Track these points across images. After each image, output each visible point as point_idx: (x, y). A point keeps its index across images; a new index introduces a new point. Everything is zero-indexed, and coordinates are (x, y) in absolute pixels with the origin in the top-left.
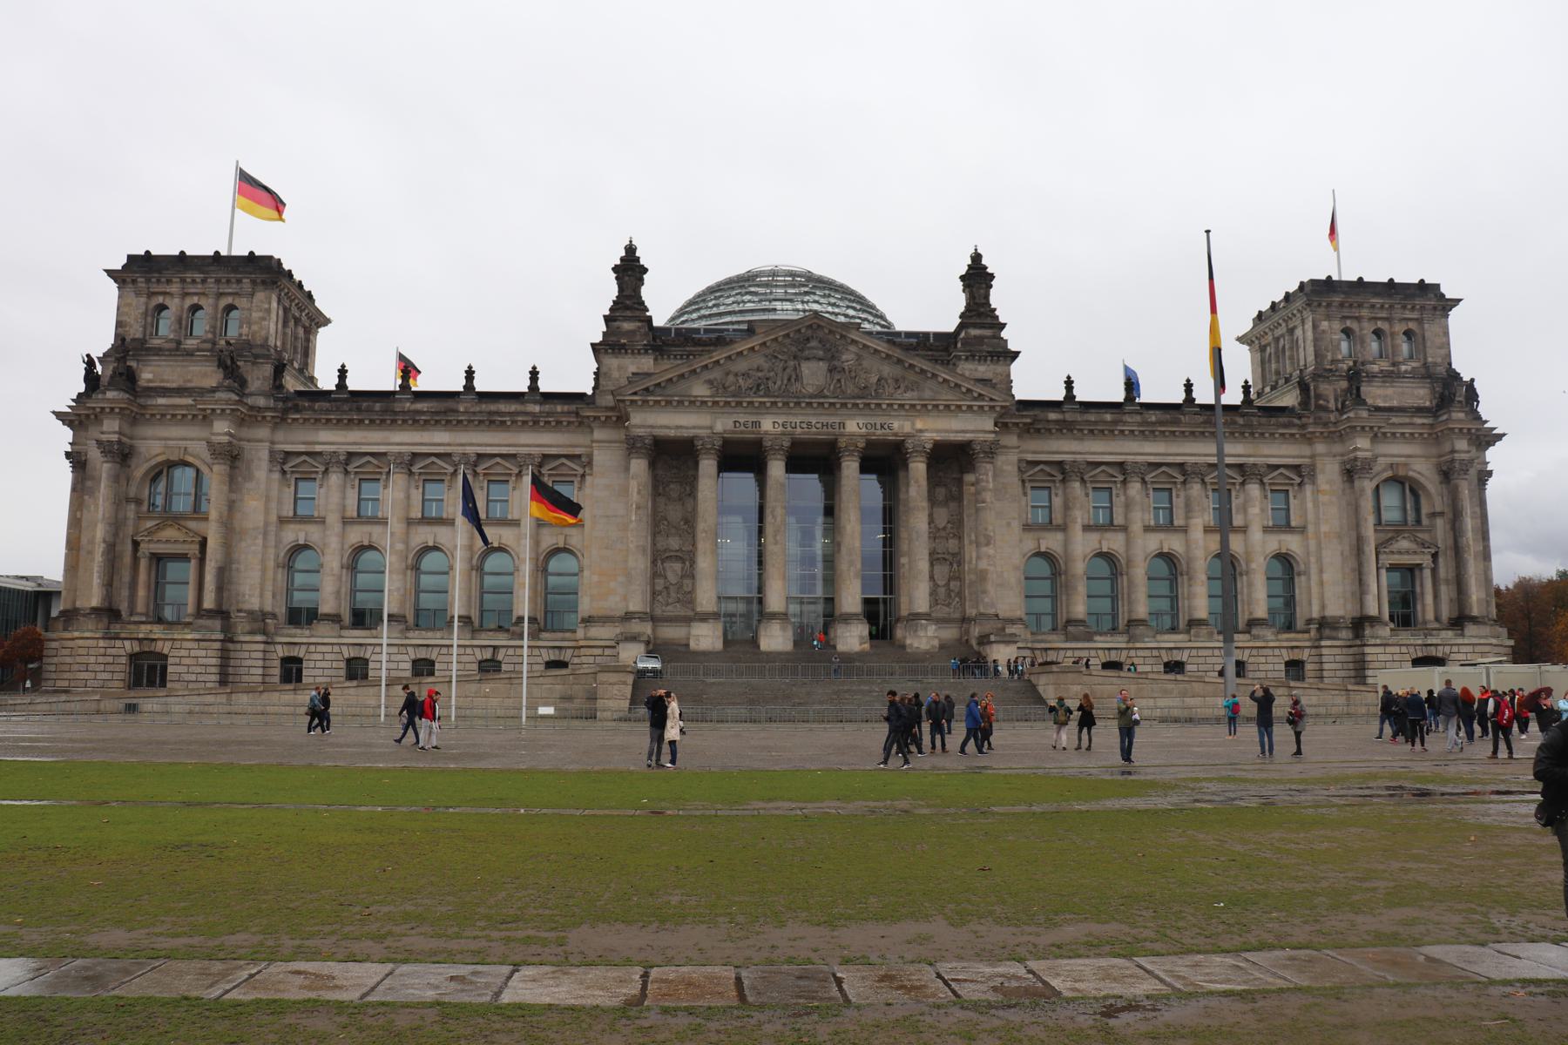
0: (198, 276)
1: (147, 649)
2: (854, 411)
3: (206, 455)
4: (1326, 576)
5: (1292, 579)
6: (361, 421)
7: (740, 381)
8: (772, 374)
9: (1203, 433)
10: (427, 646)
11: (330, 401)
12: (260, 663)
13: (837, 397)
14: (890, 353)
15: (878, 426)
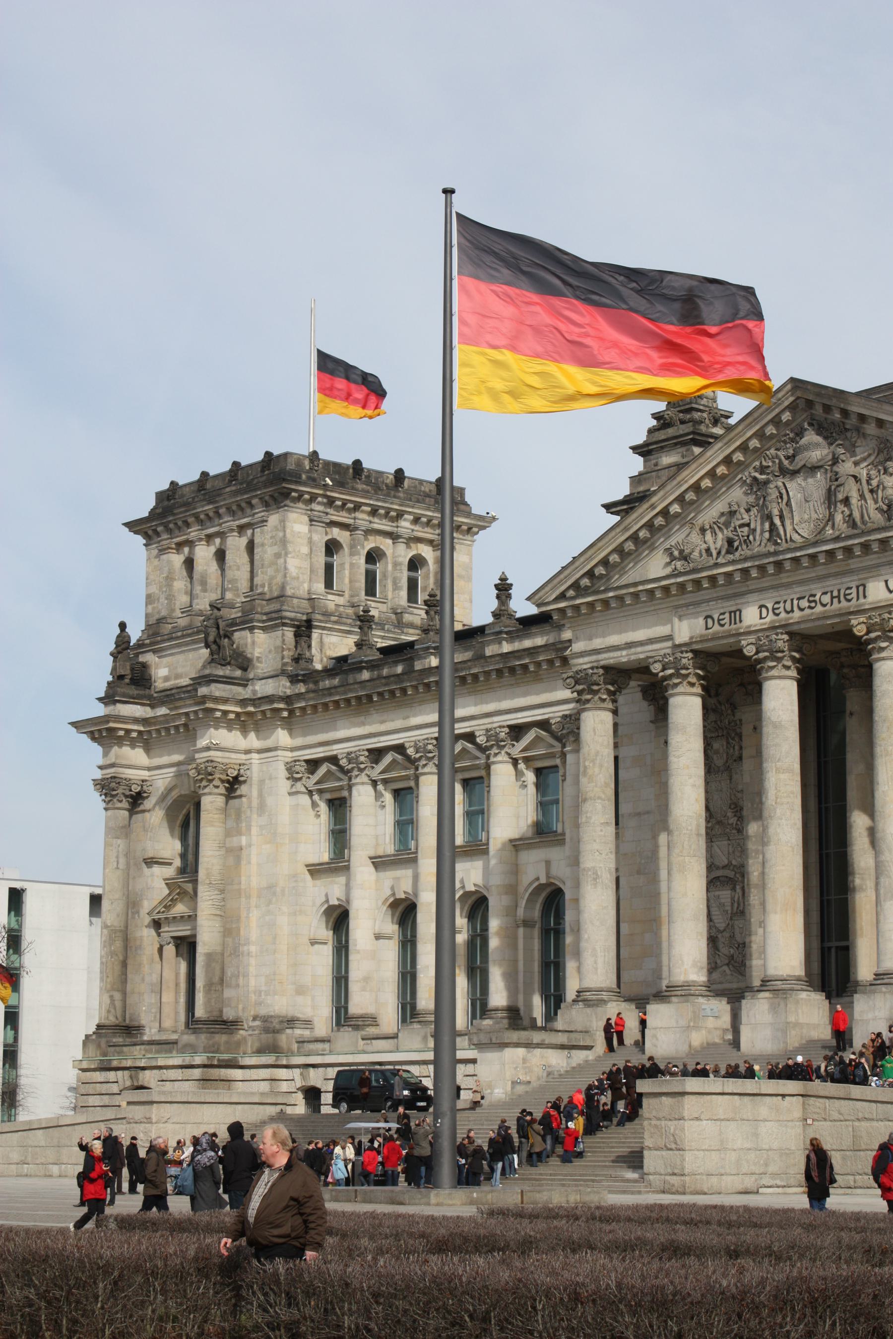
13: (837, 539)
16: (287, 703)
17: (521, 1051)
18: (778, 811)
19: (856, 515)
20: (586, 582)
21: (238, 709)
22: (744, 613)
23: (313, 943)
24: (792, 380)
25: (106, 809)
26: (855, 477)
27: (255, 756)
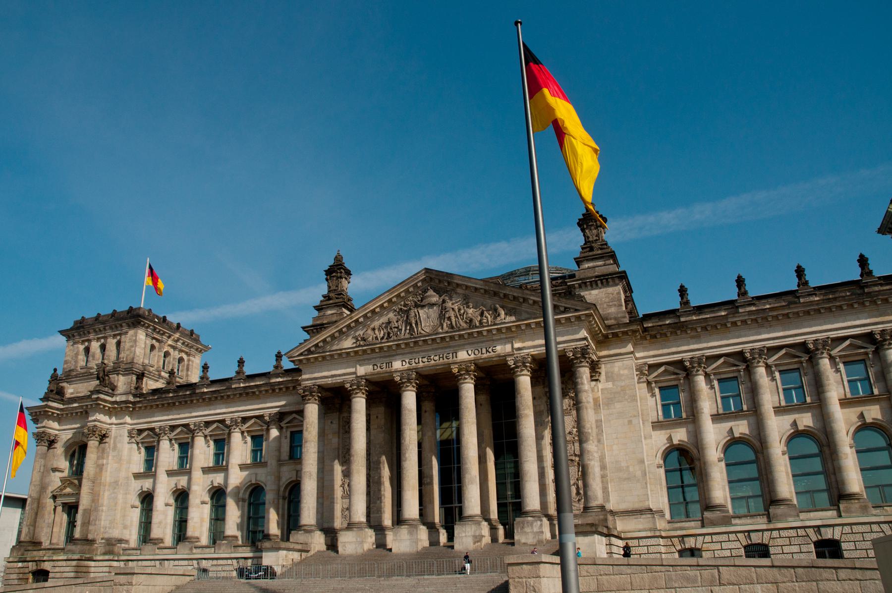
0: (101, 326)
1: (39, 568)
2: (462, 342)
7: (377, 332)
8: (400, 322)
9: (818, 311)
13: (447, 332)
14: (487, 288)
15: (484, 351)
16: (133, 405)
17: (285, 552)
18: (410, 447)
19: (454, 323)
20: (313, 349)
21: (110, 406)
22: (393, 363)
23: (133, 507)
24: (426, 269)
25: (37, 446)
26: (453, 309)
27: (114, 426)
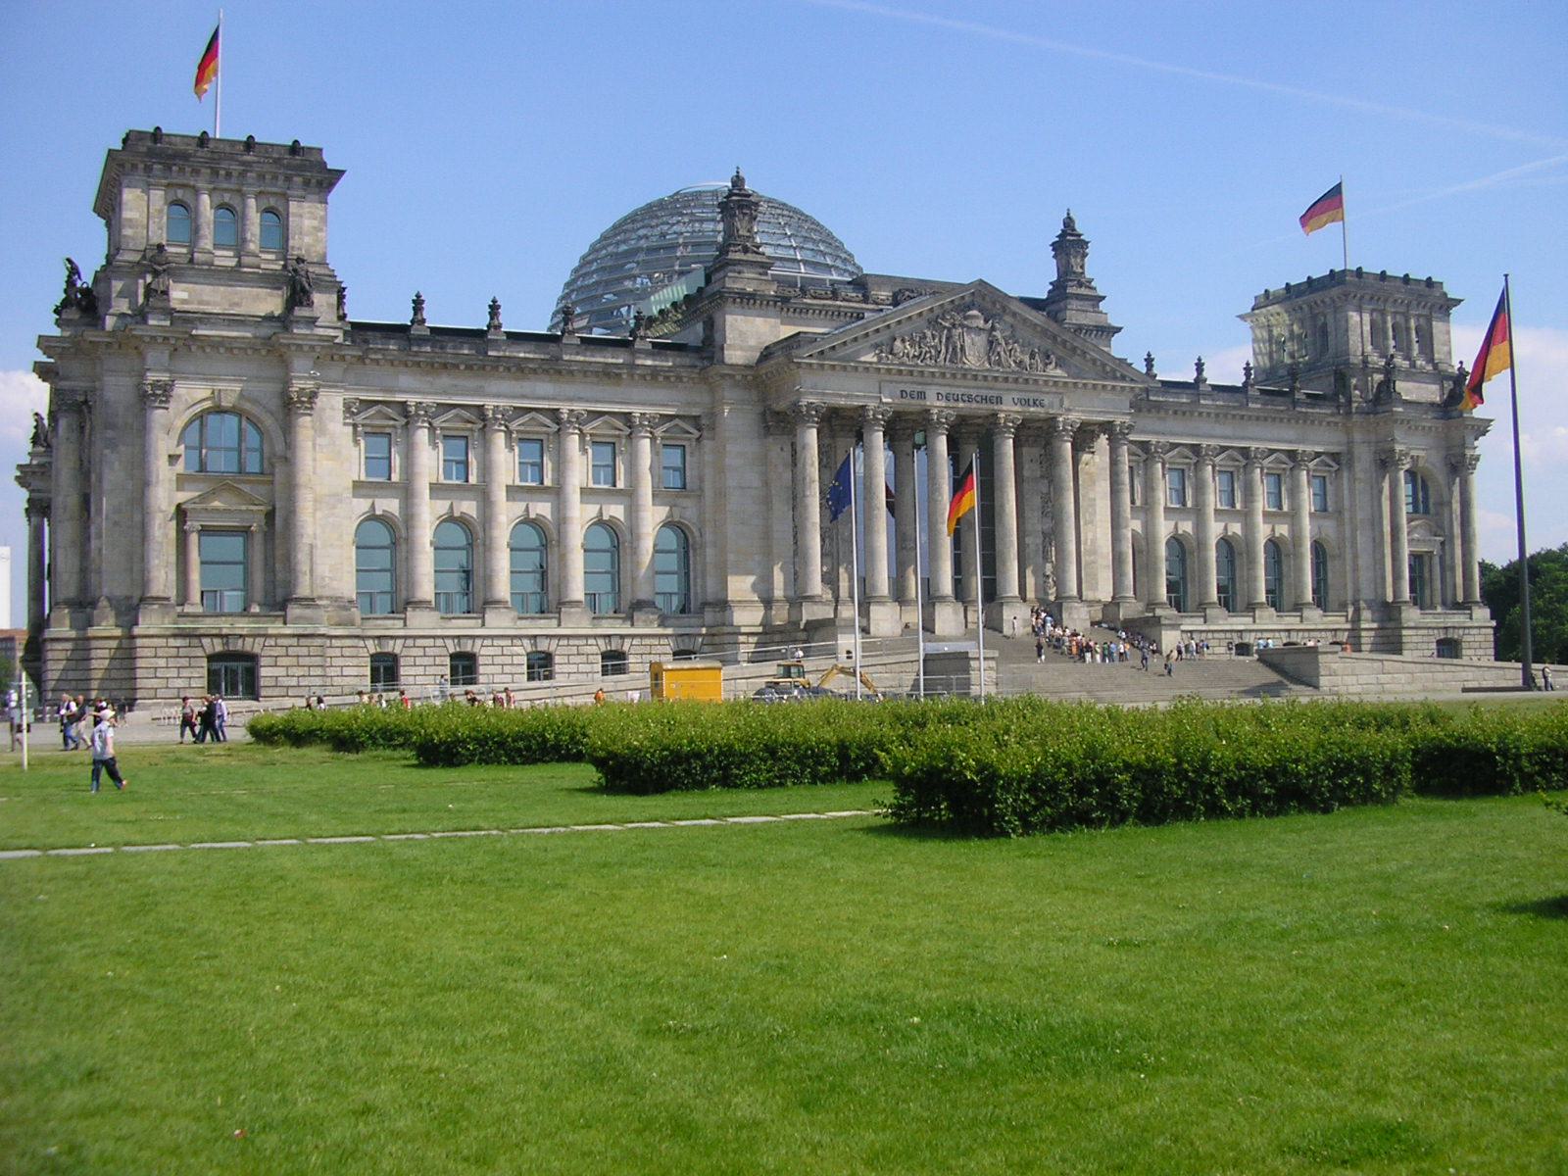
0: (235, 168)
2: (1014, 386)
3: (274, 403)
4: (1361, 562)
5: (1325, 563)
6: (456, 366)
8: (937, 340)
10: (547, 636)
11: (409, 340)
12: (355, 661)
15: (1031, 403)
